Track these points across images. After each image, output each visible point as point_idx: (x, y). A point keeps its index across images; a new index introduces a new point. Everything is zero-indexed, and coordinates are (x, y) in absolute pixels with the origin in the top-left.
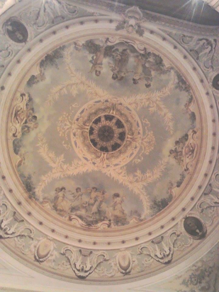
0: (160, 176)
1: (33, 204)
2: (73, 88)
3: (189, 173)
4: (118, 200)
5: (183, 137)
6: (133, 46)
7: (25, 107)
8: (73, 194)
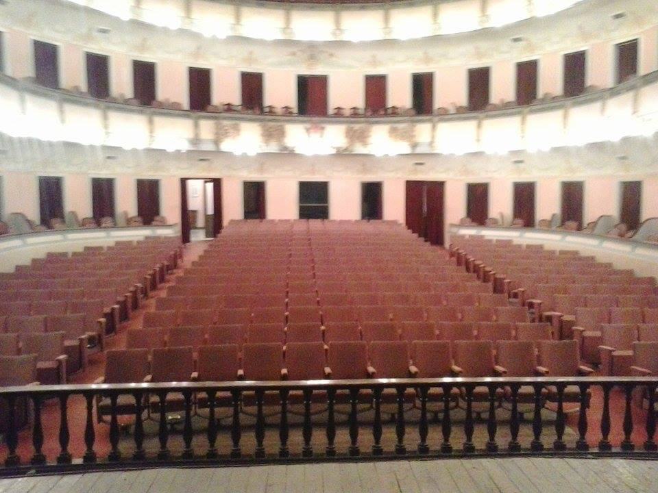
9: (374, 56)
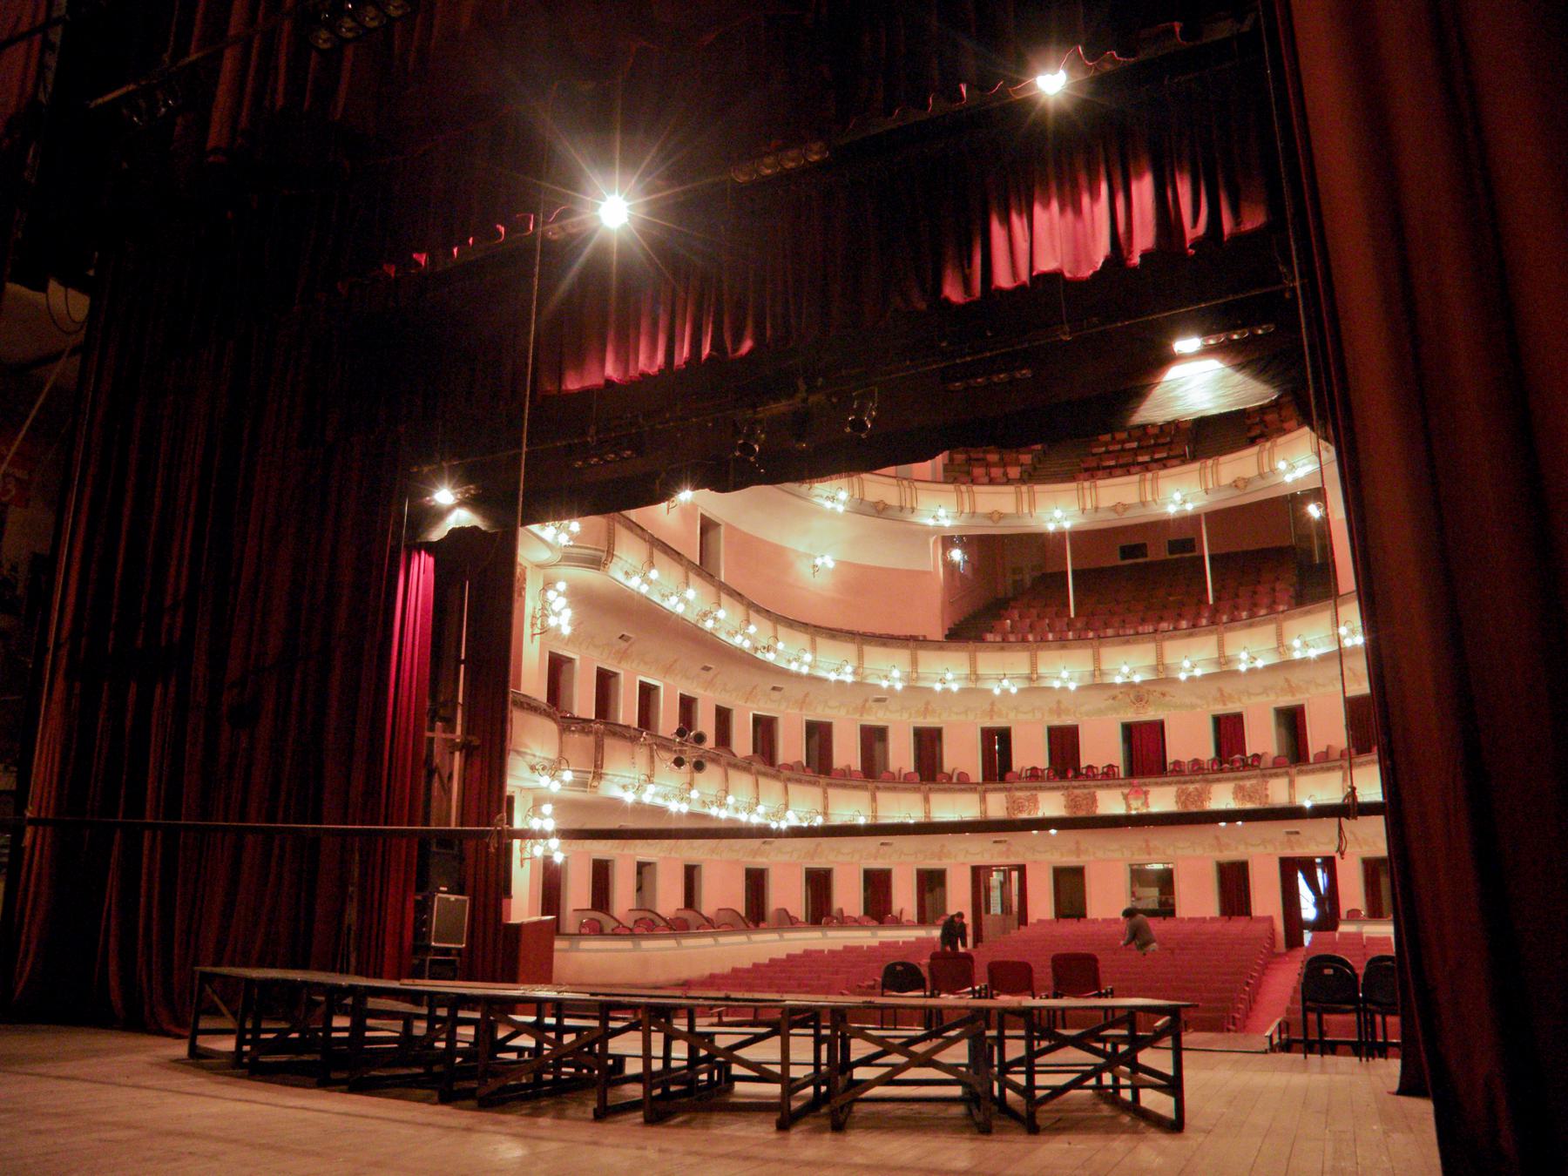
9: (1220, 690)
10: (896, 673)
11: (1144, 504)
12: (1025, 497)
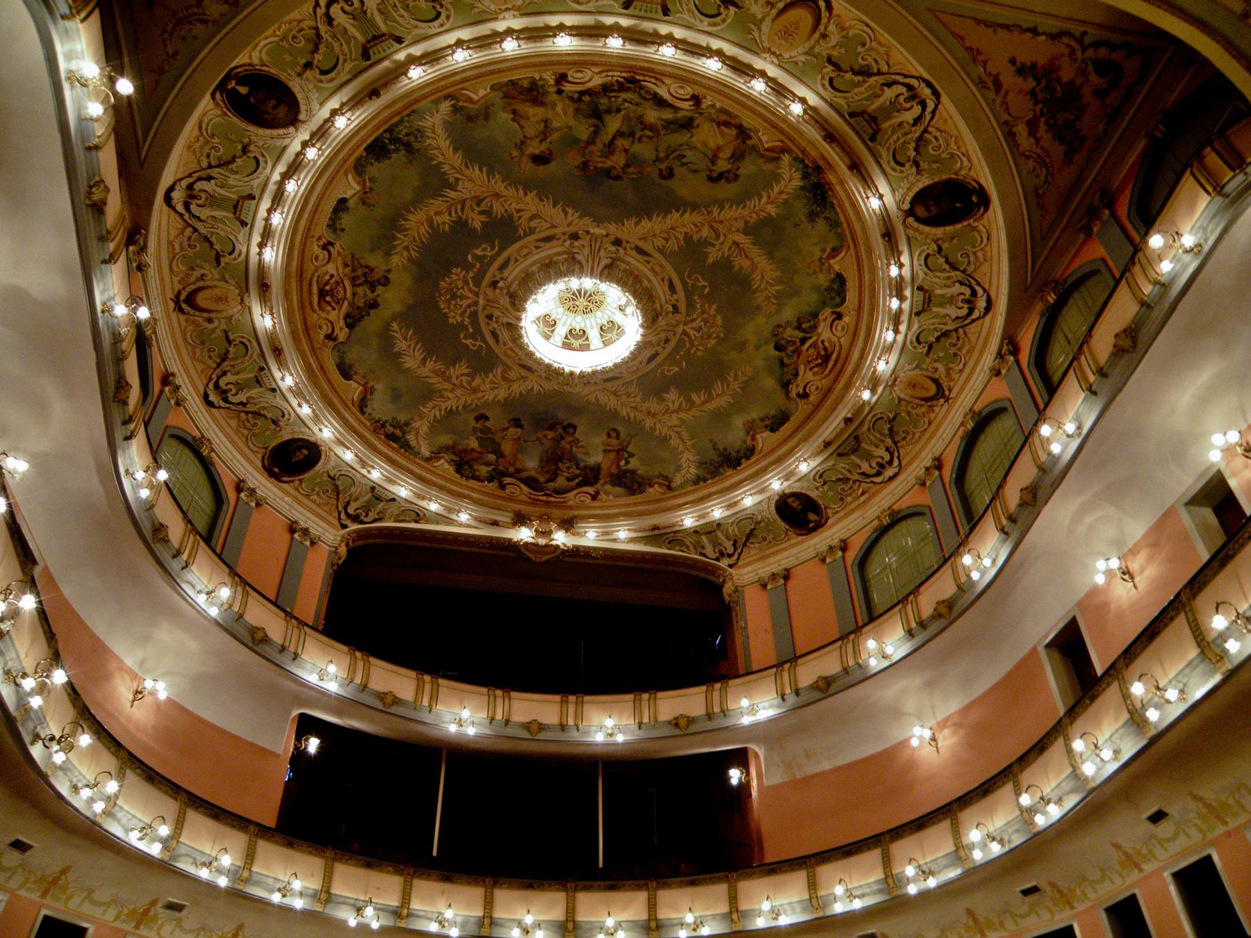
0: (406, 220)
1: (813, 154)
2: (677, 405)
3: (319, 238)
4: (534, 148)
5: (359, 320)
6: (531, 488)
7: (801, 372)
8: (683, 165)
10: (226, 861)
11: (563, 727)
12: (428, 687)
